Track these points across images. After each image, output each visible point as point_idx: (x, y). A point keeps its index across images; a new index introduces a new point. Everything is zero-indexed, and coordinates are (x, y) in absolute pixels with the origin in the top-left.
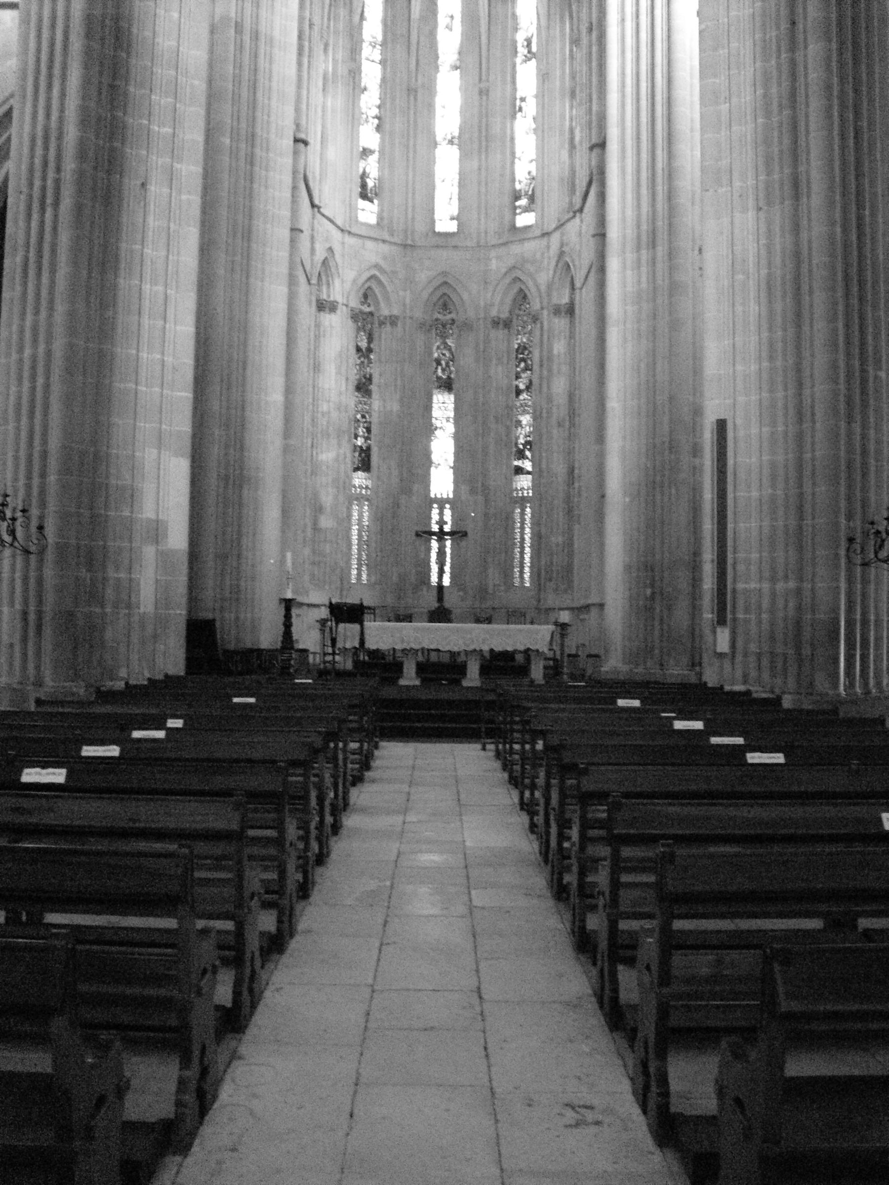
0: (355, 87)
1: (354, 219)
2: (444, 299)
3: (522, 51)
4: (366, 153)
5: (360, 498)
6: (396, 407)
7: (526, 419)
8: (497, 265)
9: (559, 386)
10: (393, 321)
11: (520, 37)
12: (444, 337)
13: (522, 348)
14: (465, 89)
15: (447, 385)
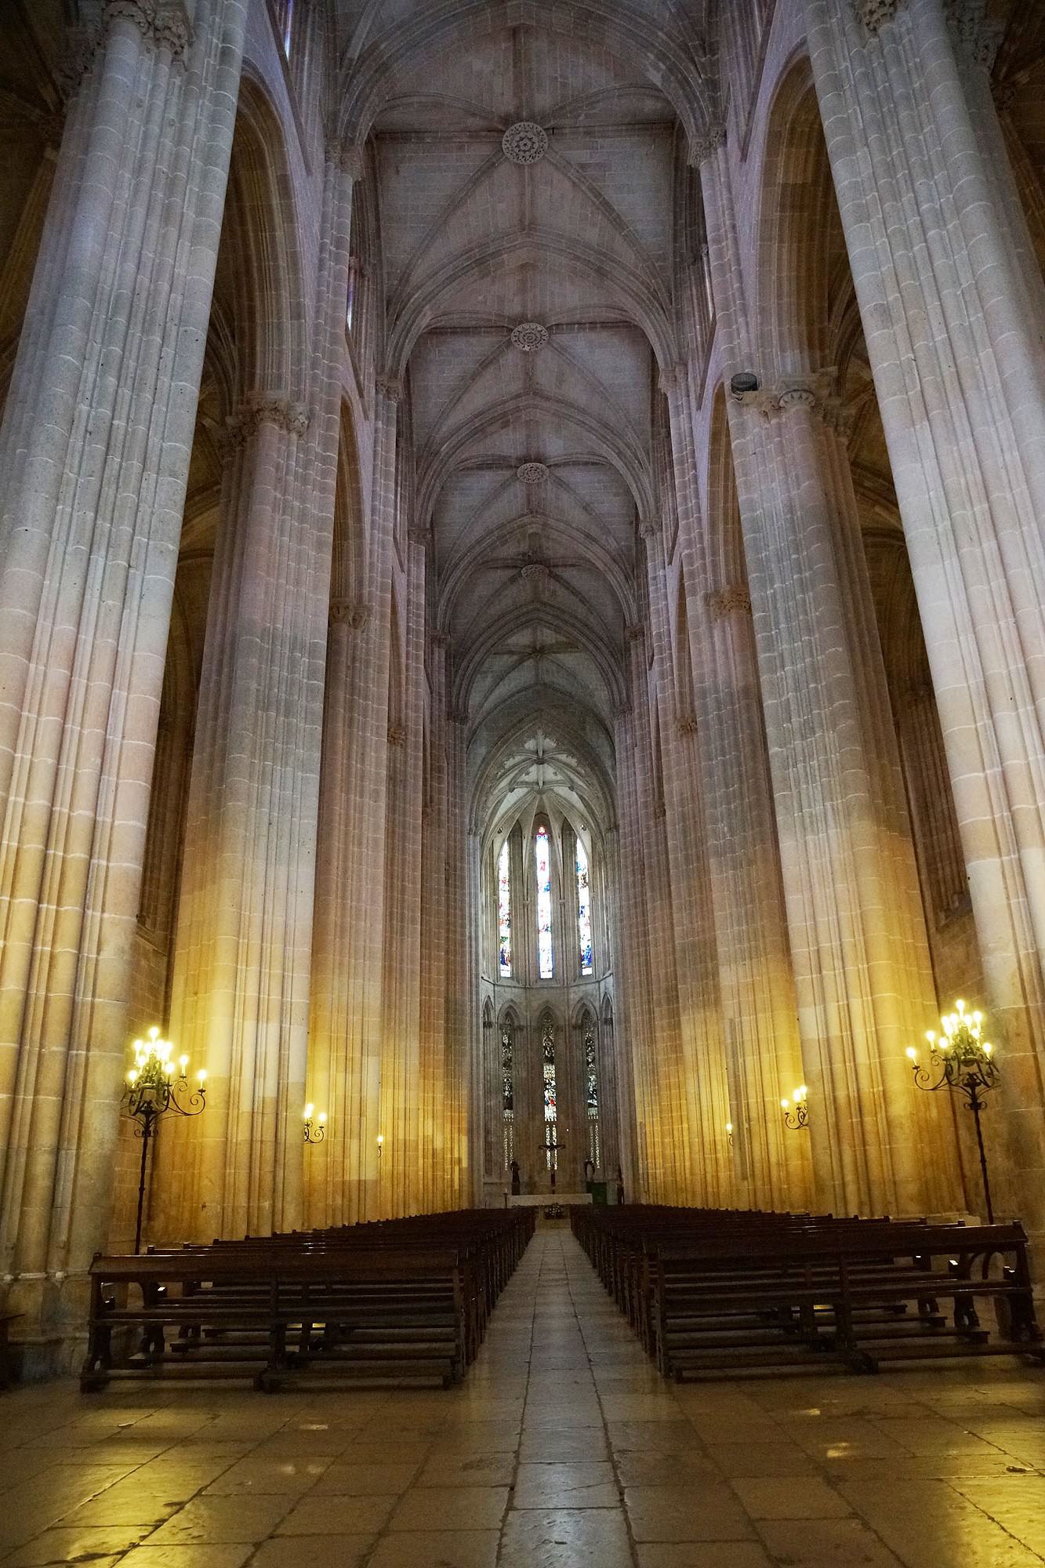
0: (496, 905)
1: (499, 977)
2: (547, 1014)
3: (581, 882)
4: (503, 939)
5: (508, 1124)
6: (524, 1075)
7: (593, 1078)
8: (574, 996)
9: (608, 1061)
10: (521, 1028)
11: (580, 874)
12: (548, 1035)
13: (589, 1040)
14: (553, 902)
15: (551, 1061)
